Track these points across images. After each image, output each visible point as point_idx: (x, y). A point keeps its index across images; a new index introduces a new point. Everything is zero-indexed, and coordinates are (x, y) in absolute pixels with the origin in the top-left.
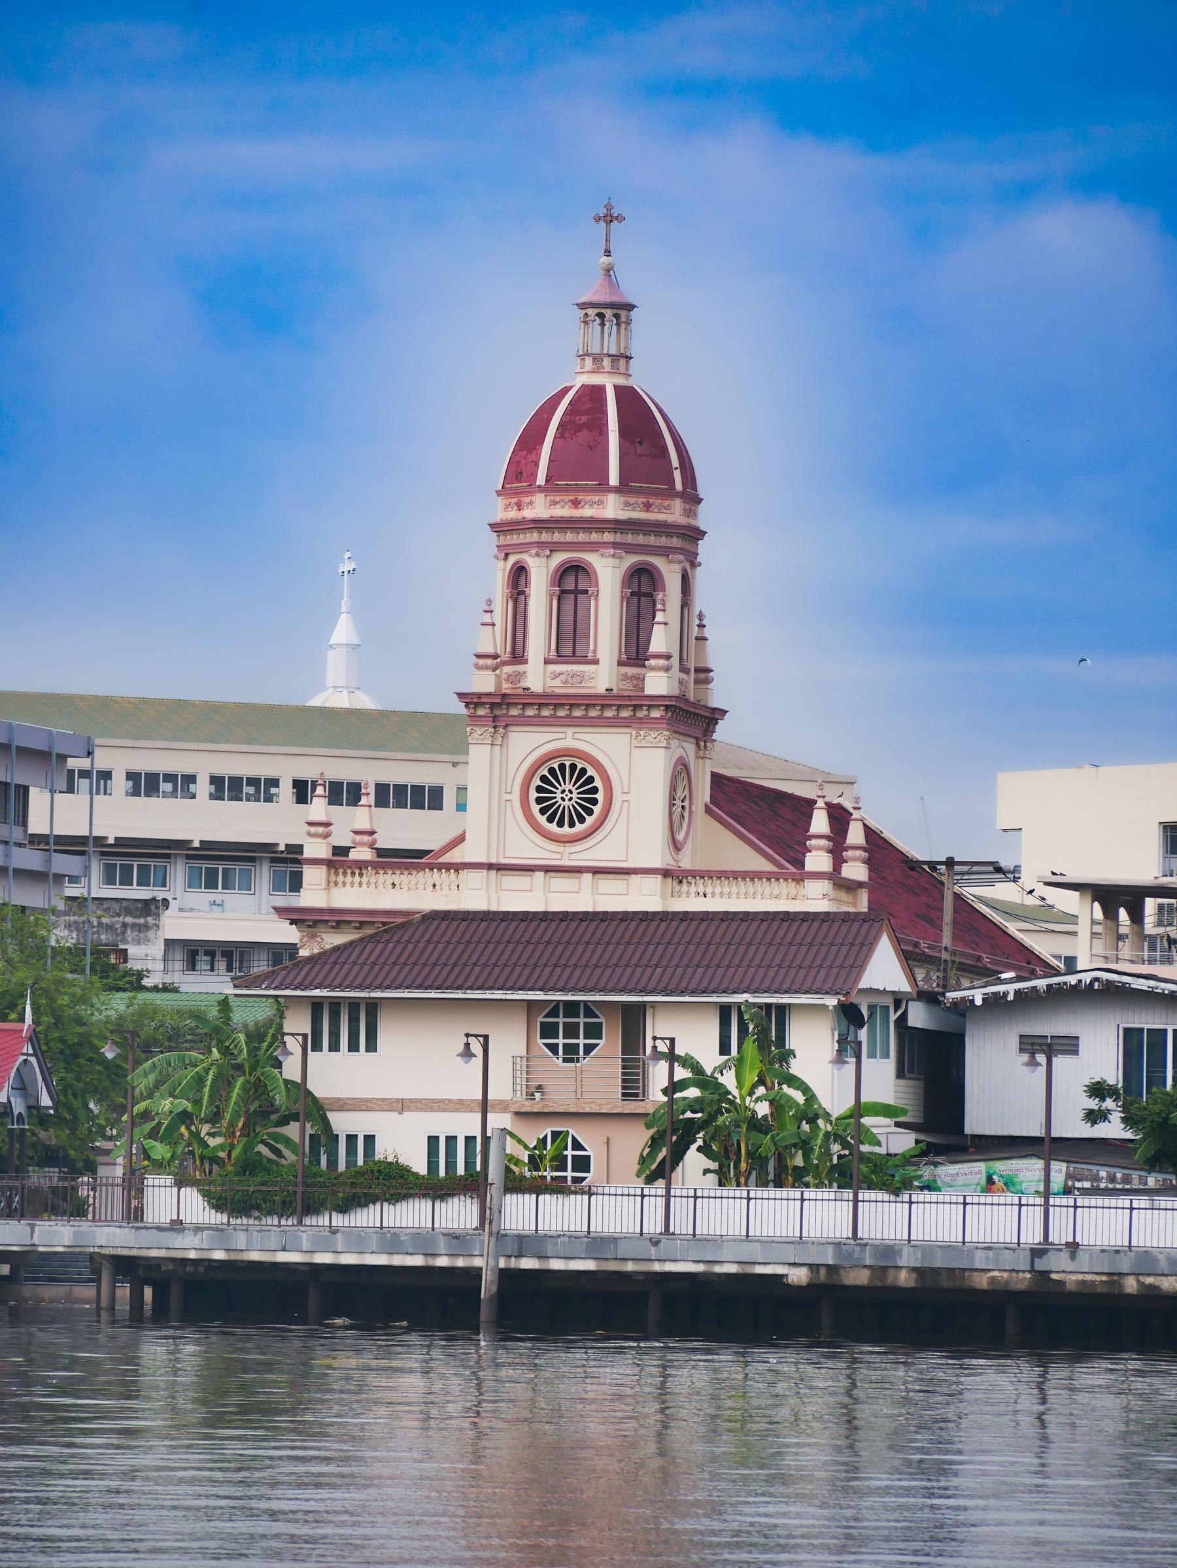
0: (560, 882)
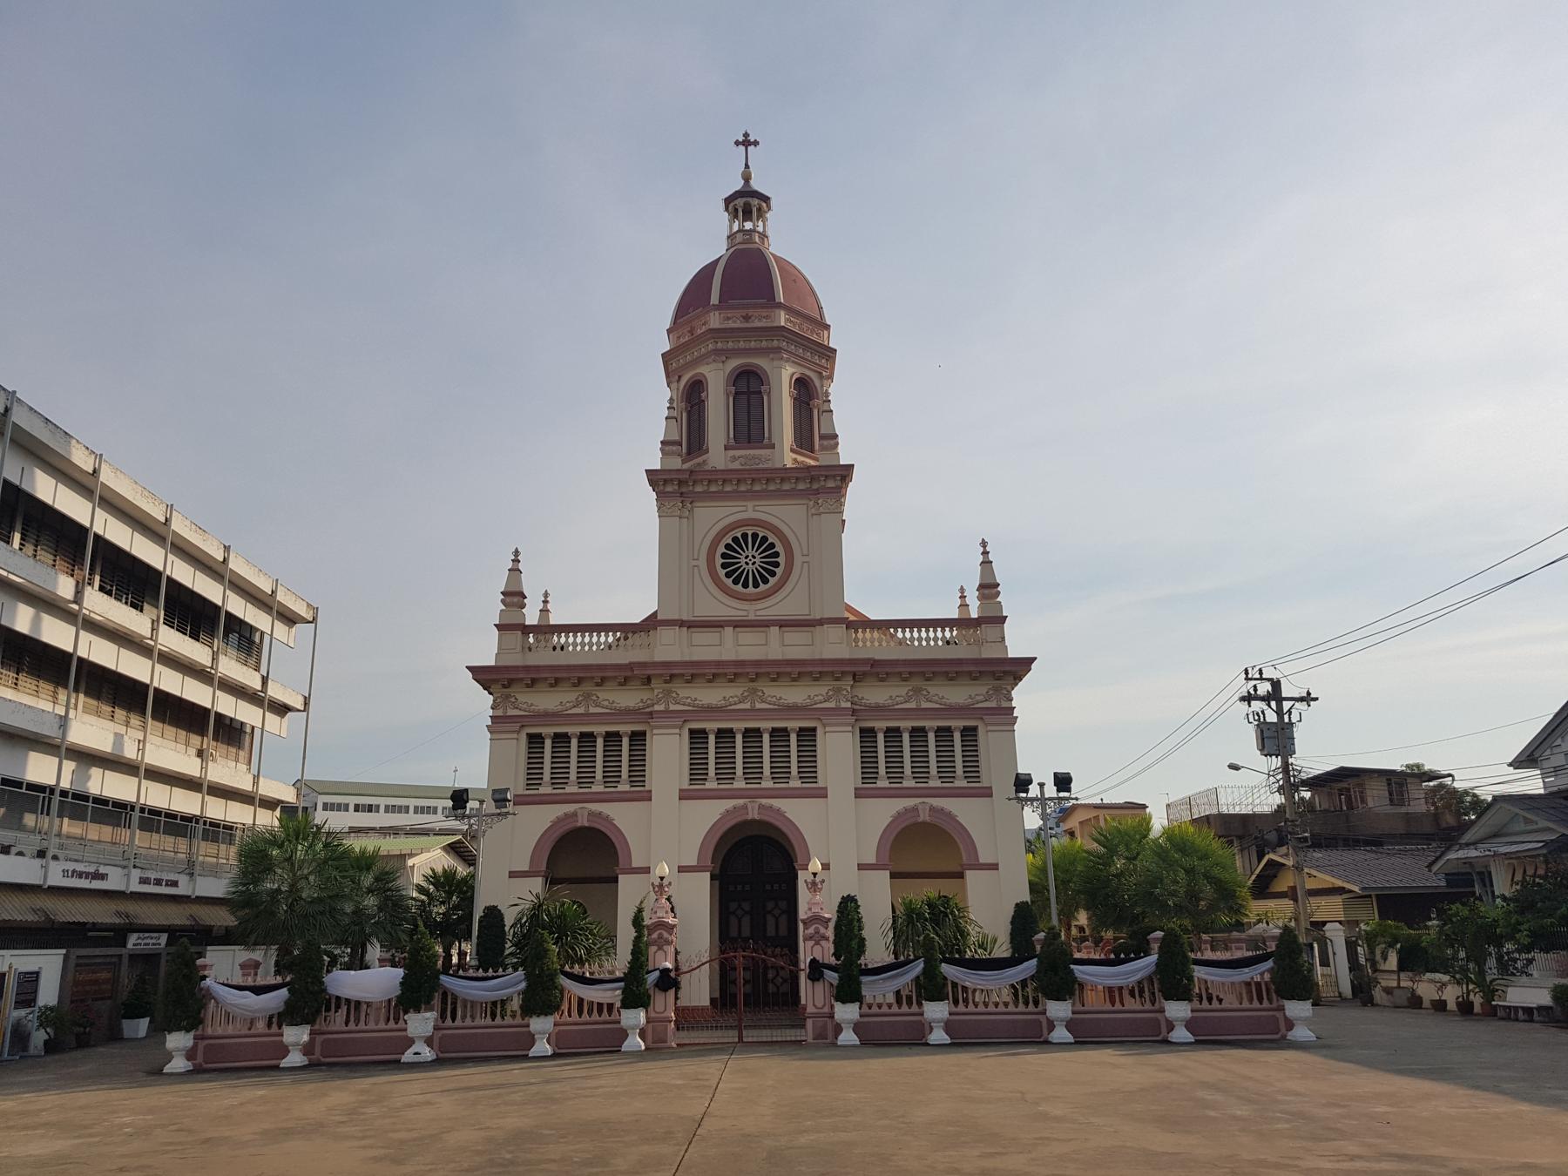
0: (747, 636)
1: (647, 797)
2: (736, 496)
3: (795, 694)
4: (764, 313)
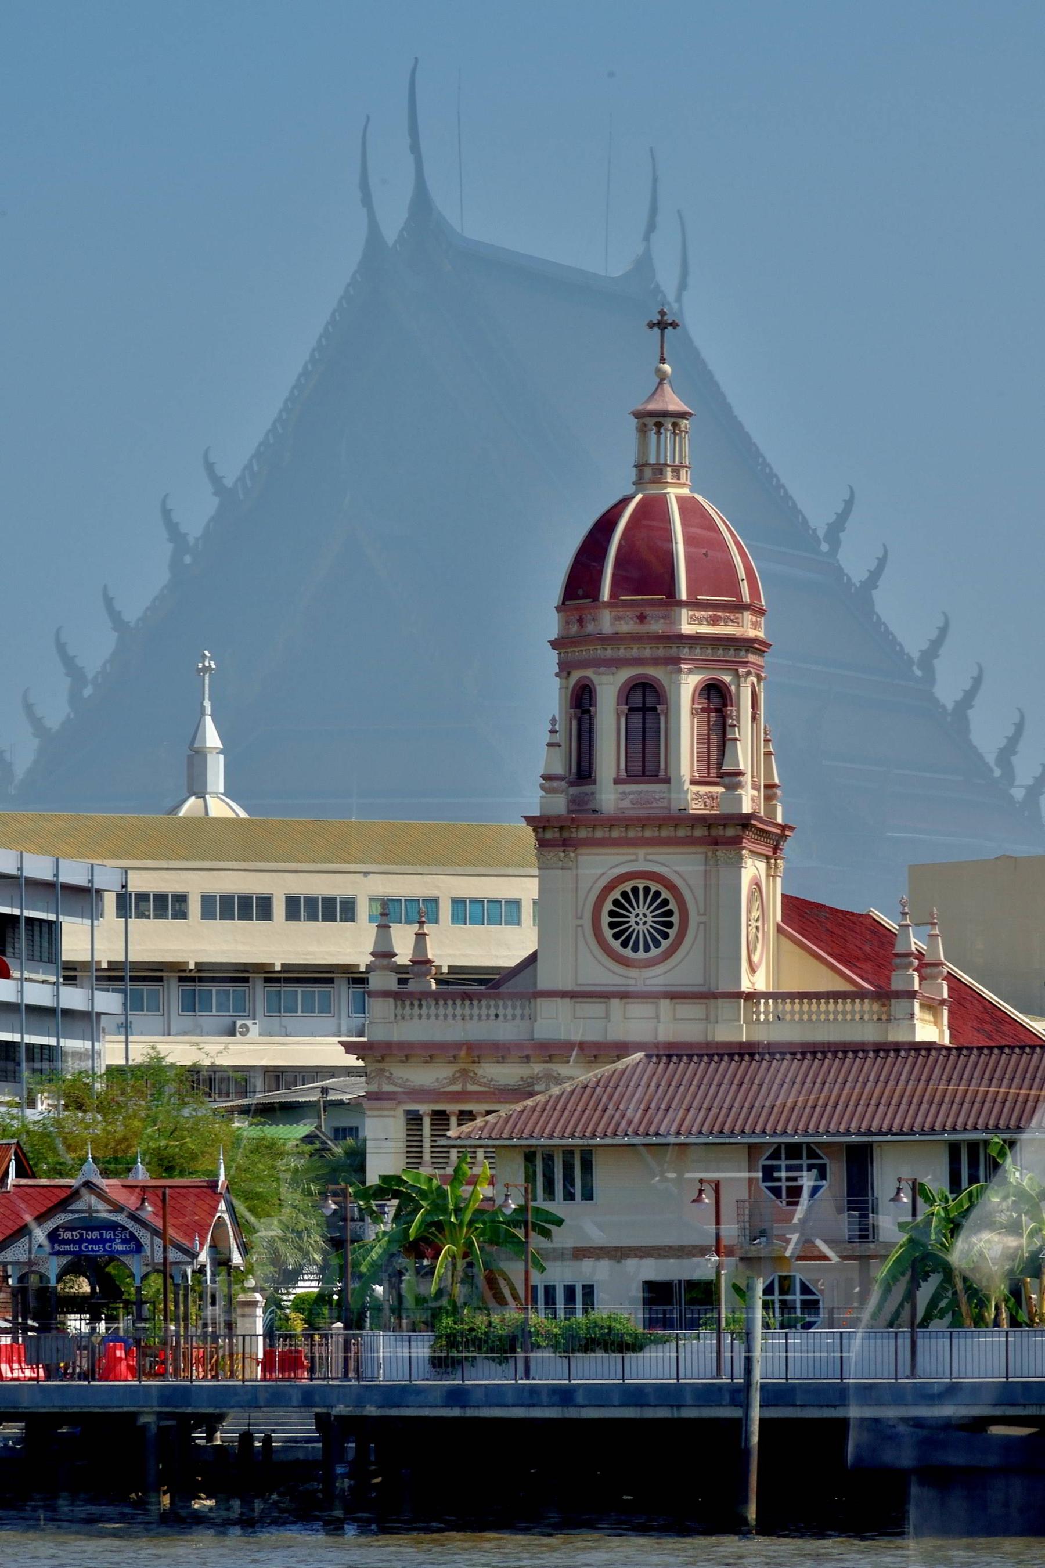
4: (660, 611)
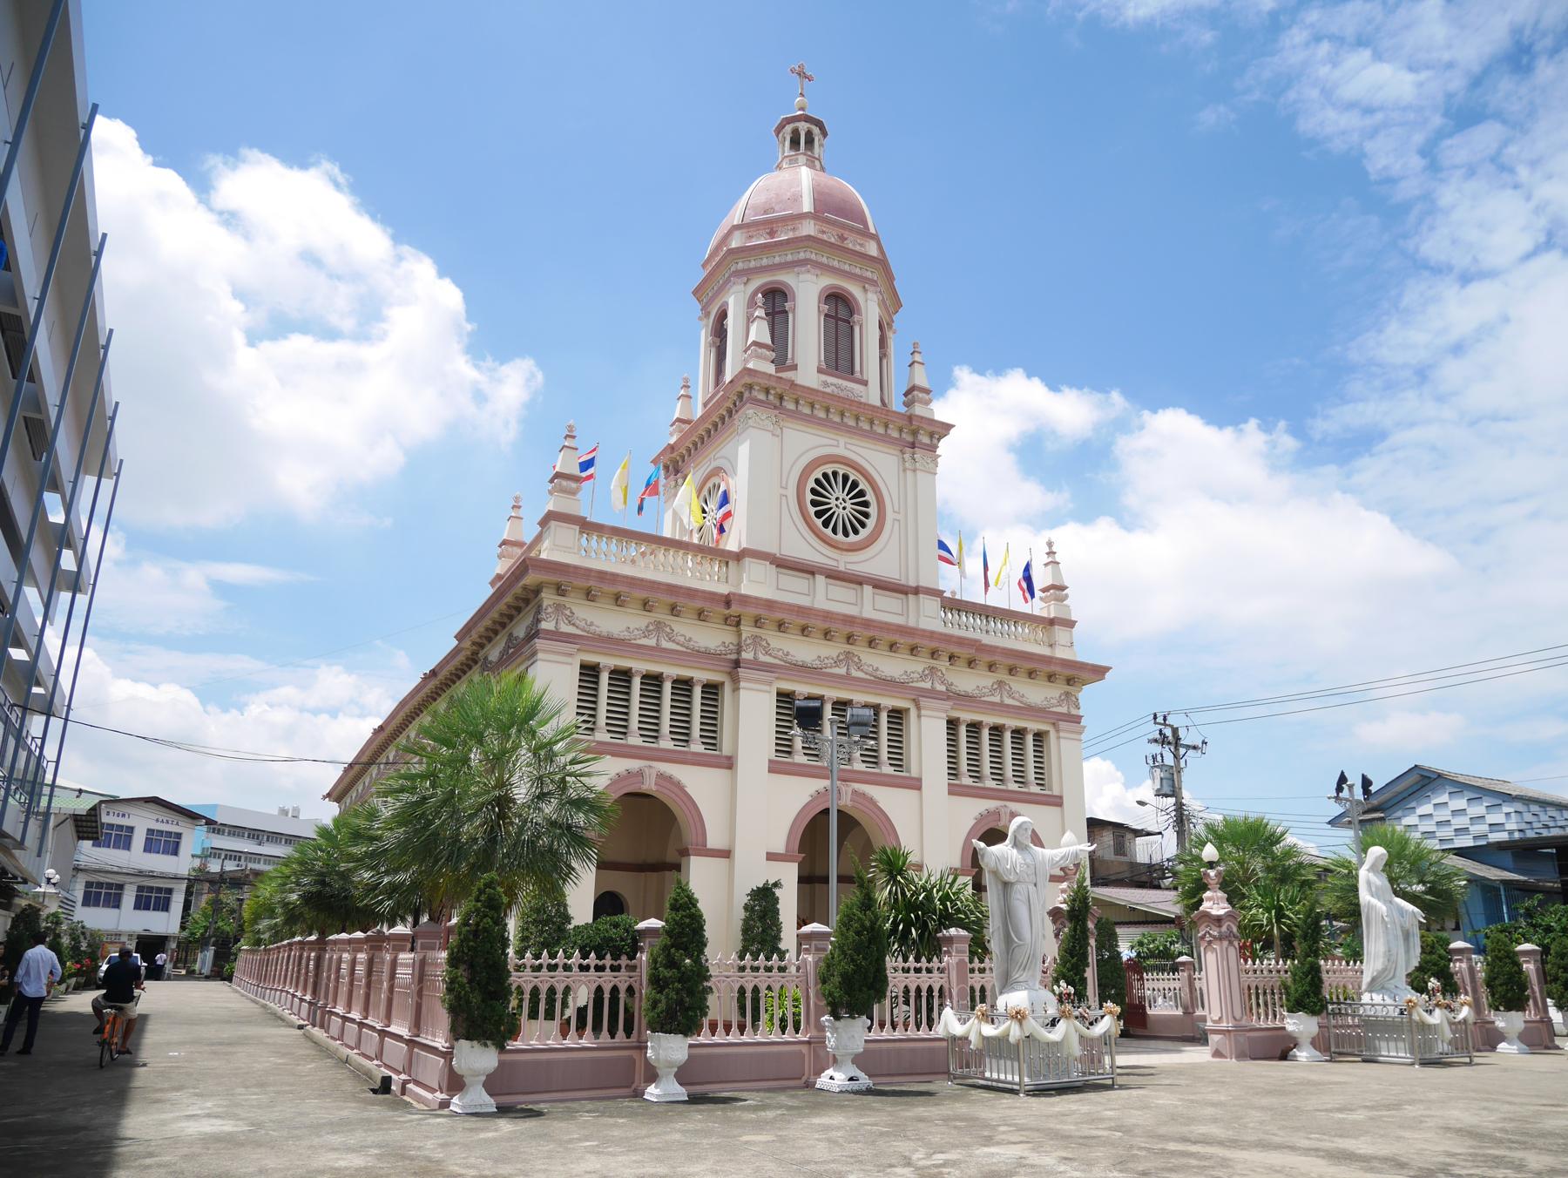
1: (729, 763)
2: (825, 424)
3: (893, 666)
